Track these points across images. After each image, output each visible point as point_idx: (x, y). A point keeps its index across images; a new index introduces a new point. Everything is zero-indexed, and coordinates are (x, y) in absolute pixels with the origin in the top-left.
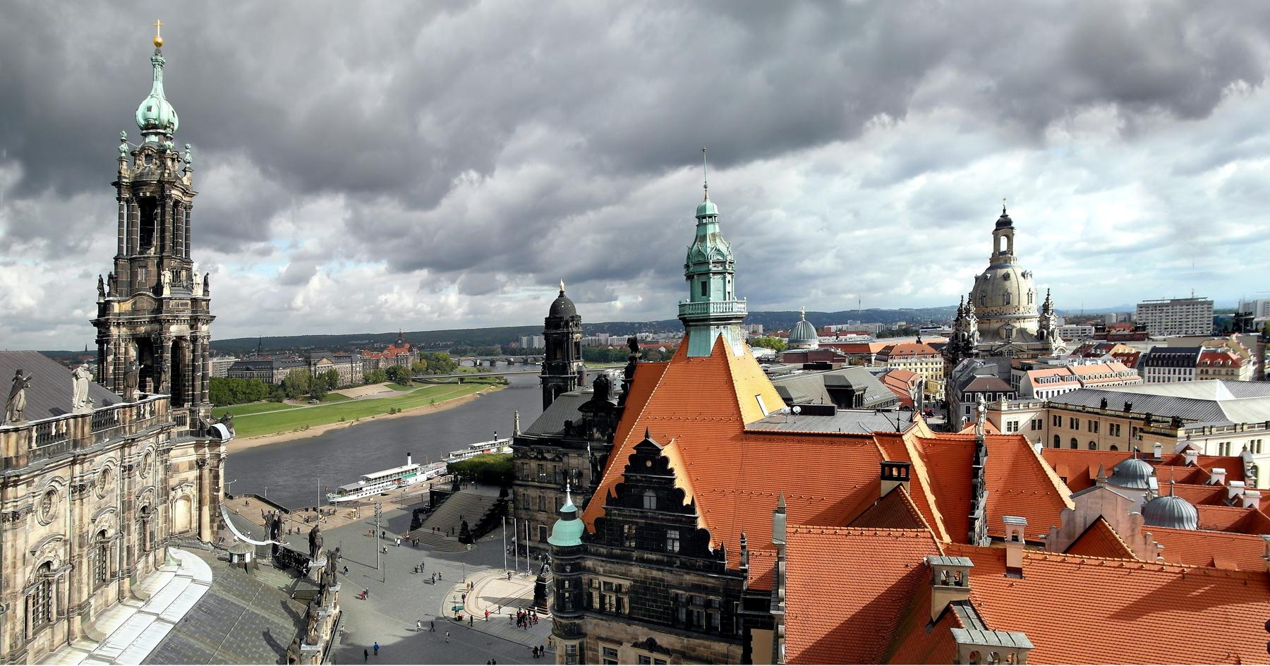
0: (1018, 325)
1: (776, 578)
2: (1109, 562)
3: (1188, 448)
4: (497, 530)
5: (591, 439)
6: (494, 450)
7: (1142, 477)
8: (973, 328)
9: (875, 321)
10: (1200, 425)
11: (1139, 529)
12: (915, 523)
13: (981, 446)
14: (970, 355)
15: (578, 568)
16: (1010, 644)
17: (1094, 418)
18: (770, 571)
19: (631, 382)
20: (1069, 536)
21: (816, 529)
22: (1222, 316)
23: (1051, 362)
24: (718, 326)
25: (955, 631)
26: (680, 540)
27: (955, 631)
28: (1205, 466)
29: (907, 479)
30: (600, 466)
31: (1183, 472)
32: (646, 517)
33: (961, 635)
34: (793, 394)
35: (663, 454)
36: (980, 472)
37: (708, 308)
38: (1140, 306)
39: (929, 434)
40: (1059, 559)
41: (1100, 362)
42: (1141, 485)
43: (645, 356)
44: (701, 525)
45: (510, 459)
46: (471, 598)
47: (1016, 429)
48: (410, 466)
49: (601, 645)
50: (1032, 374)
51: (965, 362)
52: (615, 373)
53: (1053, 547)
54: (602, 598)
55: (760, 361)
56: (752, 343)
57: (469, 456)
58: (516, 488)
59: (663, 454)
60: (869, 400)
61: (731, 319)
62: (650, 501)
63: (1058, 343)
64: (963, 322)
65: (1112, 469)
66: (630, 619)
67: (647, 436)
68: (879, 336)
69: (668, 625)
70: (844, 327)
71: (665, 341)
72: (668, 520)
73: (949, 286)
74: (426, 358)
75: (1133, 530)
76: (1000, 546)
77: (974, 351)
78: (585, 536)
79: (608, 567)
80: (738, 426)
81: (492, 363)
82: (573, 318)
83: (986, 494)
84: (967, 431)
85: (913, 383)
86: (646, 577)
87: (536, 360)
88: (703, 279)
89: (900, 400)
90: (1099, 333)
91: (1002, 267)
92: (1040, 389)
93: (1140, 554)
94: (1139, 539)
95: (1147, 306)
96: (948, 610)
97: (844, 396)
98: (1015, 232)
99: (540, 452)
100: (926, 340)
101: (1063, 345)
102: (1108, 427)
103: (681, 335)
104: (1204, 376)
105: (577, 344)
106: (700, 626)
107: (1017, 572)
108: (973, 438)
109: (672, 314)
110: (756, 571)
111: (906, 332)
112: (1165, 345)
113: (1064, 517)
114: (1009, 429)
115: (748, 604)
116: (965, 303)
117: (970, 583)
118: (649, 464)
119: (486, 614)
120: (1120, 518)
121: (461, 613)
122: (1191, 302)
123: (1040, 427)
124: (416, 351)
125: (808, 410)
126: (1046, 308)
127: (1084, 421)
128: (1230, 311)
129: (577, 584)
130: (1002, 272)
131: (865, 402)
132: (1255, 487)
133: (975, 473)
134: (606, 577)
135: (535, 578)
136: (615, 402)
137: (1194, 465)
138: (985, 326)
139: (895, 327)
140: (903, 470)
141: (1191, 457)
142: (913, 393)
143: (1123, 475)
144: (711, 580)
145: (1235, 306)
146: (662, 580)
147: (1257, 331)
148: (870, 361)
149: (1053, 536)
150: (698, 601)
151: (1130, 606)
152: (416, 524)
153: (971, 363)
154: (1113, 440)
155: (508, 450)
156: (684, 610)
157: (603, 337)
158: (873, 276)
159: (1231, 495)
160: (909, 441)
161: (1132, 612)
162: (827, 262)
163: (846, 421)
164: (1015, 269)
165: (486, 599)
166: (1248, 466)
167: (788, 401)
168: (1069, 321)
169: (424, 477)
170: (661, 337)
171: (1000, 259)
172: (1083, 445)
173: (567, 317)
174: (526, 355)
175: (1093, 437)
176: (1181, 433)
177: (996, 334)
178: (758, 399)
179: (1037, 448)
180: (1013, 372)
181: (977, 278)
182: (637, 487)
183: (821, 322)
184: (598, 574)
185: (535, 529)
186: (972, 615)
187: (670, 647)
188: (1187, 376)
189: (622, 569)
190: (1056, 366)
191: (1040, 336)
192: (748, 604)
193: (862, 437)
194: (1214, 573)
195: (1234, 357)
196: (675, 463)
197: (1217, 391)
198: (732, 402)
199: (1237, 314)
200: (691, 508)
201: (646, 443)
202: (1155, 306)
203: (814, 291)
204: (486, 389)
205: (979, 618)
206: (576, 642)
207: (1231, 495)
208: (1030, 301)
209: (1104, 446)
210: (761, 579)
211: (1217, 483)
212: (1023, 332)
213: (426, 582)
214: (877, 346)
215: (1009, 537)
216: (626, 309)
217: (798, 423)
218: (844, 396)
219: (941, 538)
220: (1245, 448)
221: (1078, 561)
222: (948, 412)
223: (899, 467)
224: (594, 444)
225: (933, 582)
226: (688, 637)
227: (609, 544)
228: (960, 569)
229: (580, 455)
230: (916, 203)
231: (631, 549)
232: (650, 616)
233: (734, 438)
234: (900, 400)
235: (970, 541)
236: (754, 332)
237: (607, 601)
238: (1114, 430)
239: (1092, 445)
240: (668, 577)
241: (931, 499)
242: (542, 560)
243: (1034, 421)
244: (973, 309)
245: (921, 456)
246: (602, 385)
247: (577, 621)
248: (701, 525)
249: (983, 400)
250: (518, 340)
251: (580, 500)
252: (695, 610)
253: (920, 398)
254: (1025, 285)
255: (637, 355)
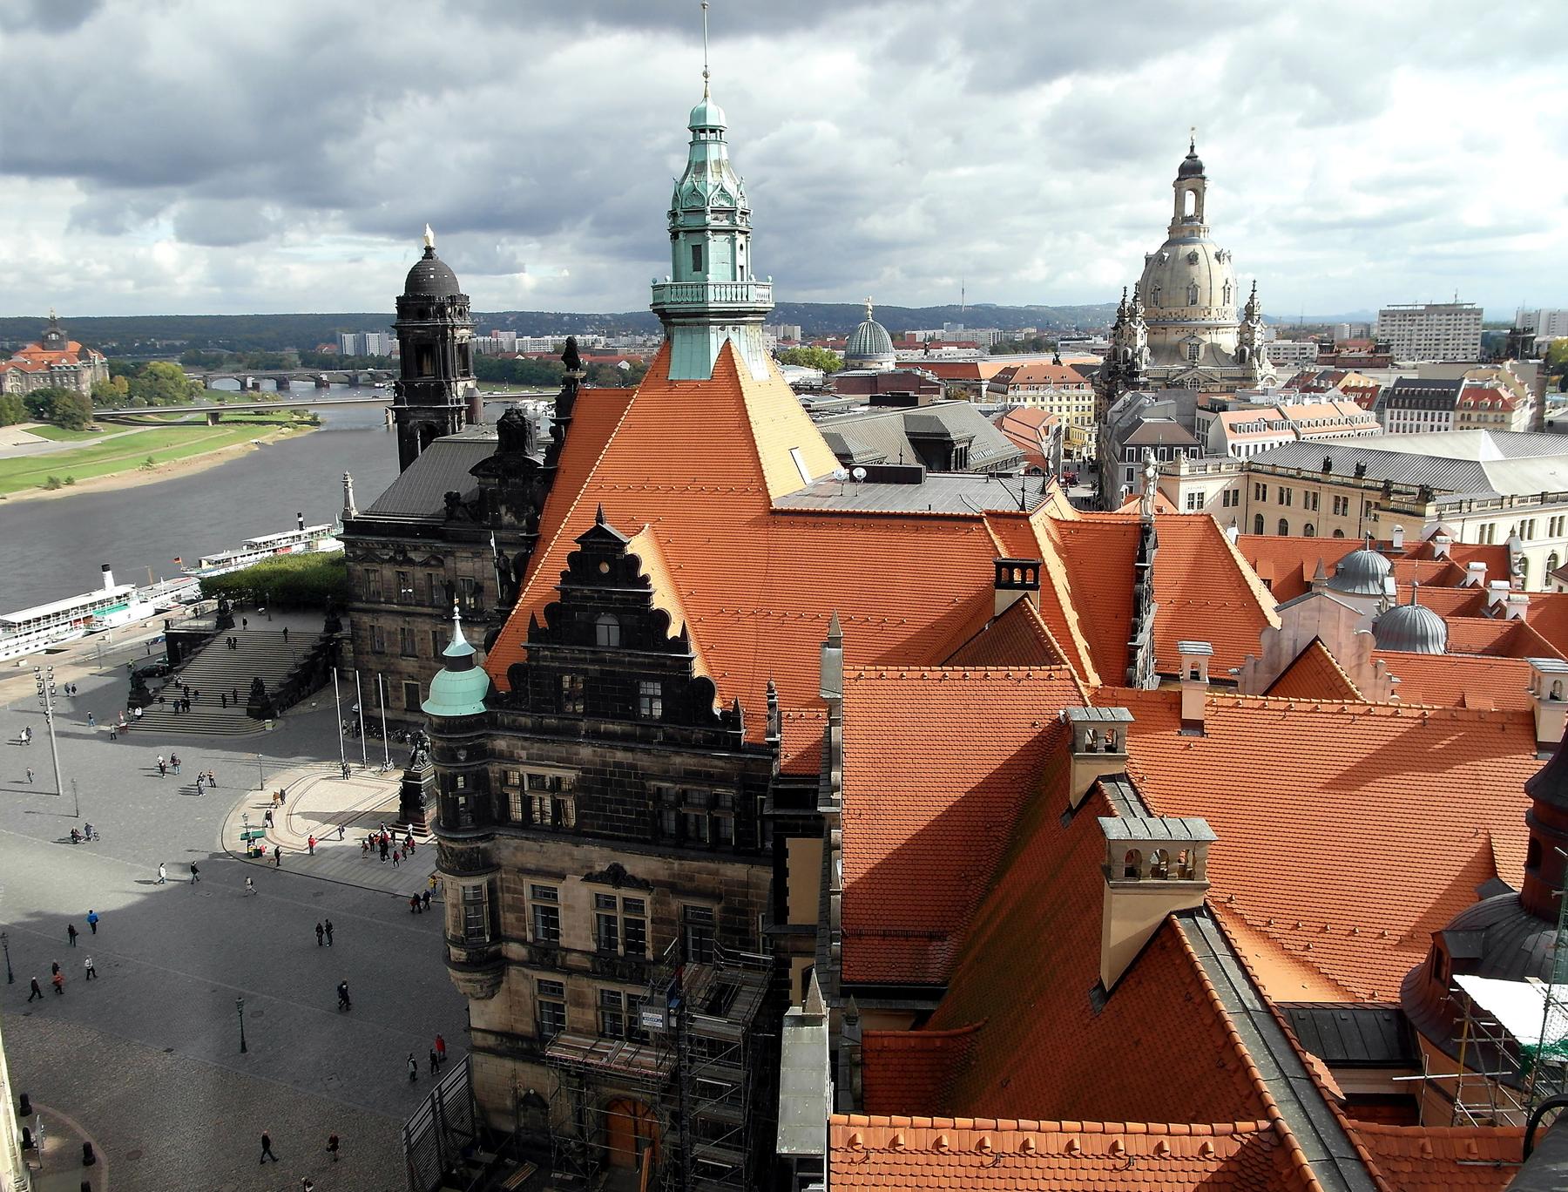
0: (1207, 338)
1: (828, 753)
2: (1327, 706)
3: (1438, 532)
4: (324, 693)
5: (497, 525)
6: (298, 548)
7: (1375, 577)
8: (1141, 342)
9: (988, 325)
10: (1456, 497)
11: (1369, 654)
12: (1045, 656)
13: (1148, 532)
14: (1135, 386)
15: (481, 753)
16: (1184, 836)
17: (1312, 488)
18: (817, 744)
19: (568, 423)
20: (1272, 669)
21: (891, 672)
22: (1493, 332)
23: (1254, 399)
24: (723, 326)
25: (1105, 821)
26: (663, 698)
27: (1105, 821)
28: (1460, 560)
29: (1034, 587)
30: (515, 573)
31: (1430, 568)
32: (602, 661)
33: (1113, 828)
34: (854, 448)
35: (629, 550)
36: (1147, 573)
37: (704, 294)
38: (1384, 314)
39: (1070, 514)
40: (1257, 704)
41: (1324, 400)
42: (1374, 589)
43: (592, 376)
44: (699, 670)
45: (335, 562)
46: (279, 815)
47: (1201, 505)
48: (111, 589)
49: (527, 883)
50: (1226, 418)
51: (1128, 396)
52: (538, 407)
53: (1249, 687)
54: (527, 803)
55: (797, 389)
56: (784, 358)
57: (244, 561)
58: (356, 616)
59: (629, 550)
60: (976, 458)
61: (745, 314)
62: (608, 632)
63: (1265, 369)
64: (1126, 329)
65: (1334, 566)
66: (577, 835)
67: (600, 519)
68: (995, 350)
69: (645, 842)
70: (938, 333)
71: (630, 350)
72: (642, 665)
73: (1106, 273)
74: (126, 372)
75: (1360, 656)
76: (1173, 688)
77: (1142, 379)
78: (491, 698)
79: (536, 749)
80: (759, 500)
81: (282, 385)
82: (453, 300)
83: (1154, 608)
84: (1128, 509)
85: (1047, 429)
86: (605, 764)
87: (375, 378)
88: (696, 240)
89: (1026, 458)
90: (1326, 354)
91: (1187, 242)
92: (1237, 442)
93: (1369, 692)
94: (1368, 669)
95: (1392, 314)
96: (1094, 790)
97: (937, 451)
98: (1208, 184)
99: (404, 552)
100: (1068, 359)
101: (1273, 371)
102: (1332, 501)
103: (656, 339)
104: (1466, 424)
105: (463, 349)
106: (701, 840)
107: (1197, 726)
108: (1137, 519)
109: (641, 303)
110: (793, 744)
111: (1037, 346)
112: (1414, 376)
113: (1265, 640)
114: (1191, 505)
115: (781, 799)
116: (1129, 299)
117: (1128, 747)
118: (605, 568)
119: (311, 843)
120: (1344, 641)
121: (258, 844)
122: (1453, 310)
123: (1235, 503)
124: (97, 358)
125: (879, 475)
126: (1249, 312)
127: (1298, 491)
128: (1505, 326)
129: (479, 781)
130: (1186, 250)
131: (971, 461)
132: (1522, 590)
133: (1138, 576)
134: (531, 768)
135: (401, 774)
136: (539, 459)
137: (1445, 558)
138: (1158, 339)
139: (1019, 337)
140: (1029, 571)
141: (1442, 547)
142: (1047, 446)
143: (1350, 575)
144: (719, 761)
145: (1510, 317)
146: (633, 767)
147: (1537, 357)
148: (978, 392)
149: (1250, 669)
150: (696, 798)
151: (1352, 770)
152: (139, 696)
153: (1136, 398)
154: (1338, 522)
155: (331, 545)
156: (673, 815)
157: (505, 338)
158: (985, 247)
159: (1491, 603)
160: (1040, 524)
161: (1350, 780)
162: (910, 221)
163: (940, 493)
164: (1206, 247)
165: (308, 816)
166: (1515, 558)
167: (845, 458)
168: (1282, 334)
169: (148, 609)
170: (622, 342)
171: (1184, 228)
172: (1296, 531)
173: (440, 297)
174: (356, 372)
175: (1310, 516)
176: (1430, 510)
177: (1174, 352)
178: (796, 455)
179: (1231, 535)
180: (1200, 414)
181: (1148, 259)
182: (585, 609)
183: (900, 323)
184: (518, 761)
185: (397, 688)
186: (1131, 796)
187: (649, 878)
188: (1443, 424)
189: (561, 751)
190: (1260, 406)
191: (1240, 358)
192: (781, 799)
193: (965, 518)
194: (1465, 716)
195: (1506, 395)
196: (651, 566)
197: (1480, 446)
198: (749, 465)
199: (1514, 331)
200: (681, 644)
201: (598, 532)
202: (1404, 314)
203: (887, 271)
204: (270, 436)
205: (1140, 800)
206: (482, 881)
207: (1491, 603)
208: (1226, 300)
209: (1324, 532)
210: (801, 756)
211: (1475, 584)
212: (1214, 349)
213: (185, 792)
214: (990, 368)
215: (1186, 674)
216: (539, 291)
217: (862, 497)
218: (937, 451)
219: (1086, 679)
220: (1513, 532)
221: (1283, 706)
222: (1097, 480)
223: (1023, 568)
224: (503, 534)
225: (1073, 748)
226: (680, 858)
227: (536, 709)
228: (1113, 726)
229: (476, 555)
230: (1056, 125)
231: (578, 717)
232: (613, 828)
233: (754, 523)
234: (1026, 458)
235: (1129, 682)
236: (787, 339)
237: (536, 806)
238: (1341, 505)
239: (1309, 529)
240: (644, 761)
241: (1072, 617)
242: (414, 742)
243: (1227, 493)
244: (1141, 310)
245: (1059, 550)
246: (514, 429)
247: (482, 845)
248: (699, 670)
249: (1152, 460)
250: (334, 340)
251: (480, 634)
252: (692, 813)
253: (1057, 455)
254: (1221, 273)
255: (571, 371)
